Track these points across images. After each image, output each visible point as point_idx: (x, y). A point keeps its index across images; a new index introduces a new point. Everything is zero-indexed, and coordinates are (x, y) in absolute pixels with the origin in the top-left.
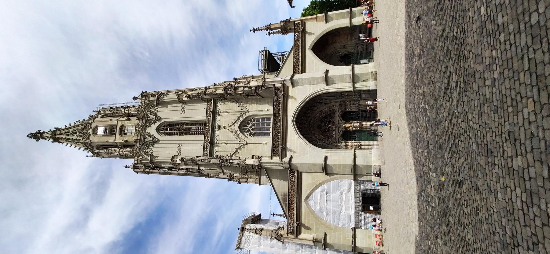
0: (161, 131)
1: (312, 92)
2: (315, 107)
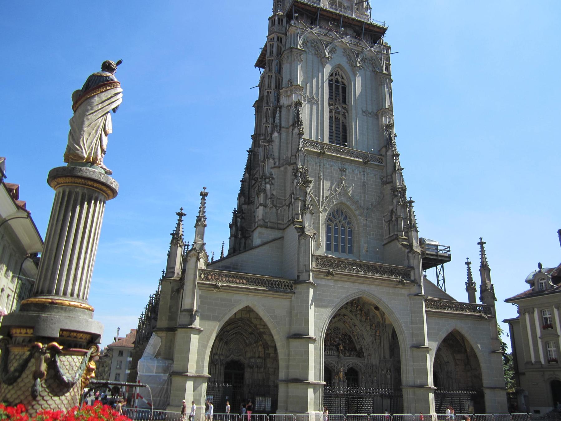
0: (336, 72)
1: (403, 325)
2: (369, 326)
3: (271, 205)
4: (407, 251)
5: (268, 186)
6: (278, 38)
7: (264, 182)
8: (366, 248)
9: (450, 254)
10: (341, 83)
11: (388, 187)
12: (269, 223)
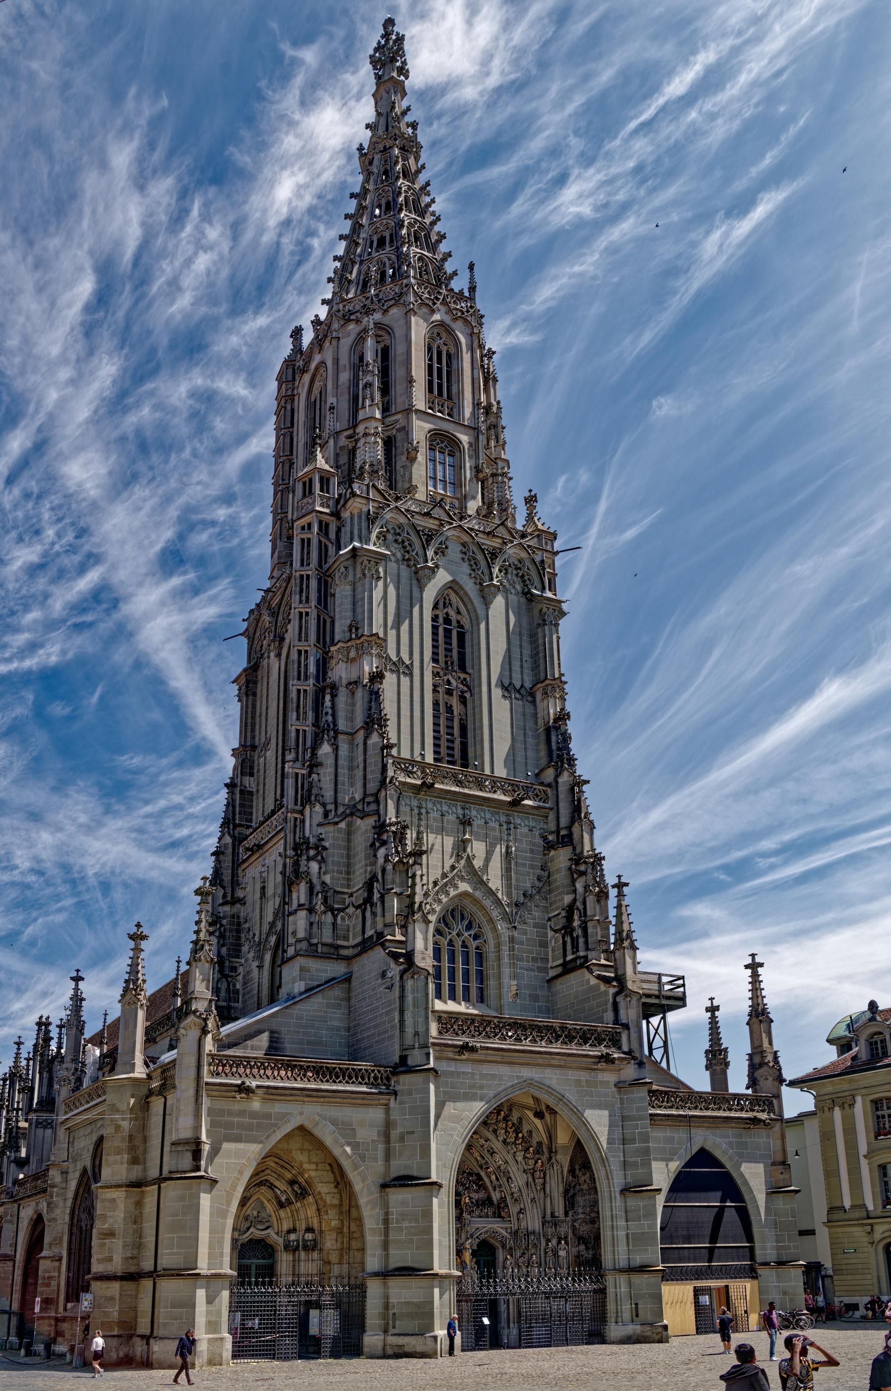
3: (323, 908)
5: (314, 866)
6: (320, 522)
7: (304, 857)
9: (684, 993)
10: (454, 623)
11: (562, 857)
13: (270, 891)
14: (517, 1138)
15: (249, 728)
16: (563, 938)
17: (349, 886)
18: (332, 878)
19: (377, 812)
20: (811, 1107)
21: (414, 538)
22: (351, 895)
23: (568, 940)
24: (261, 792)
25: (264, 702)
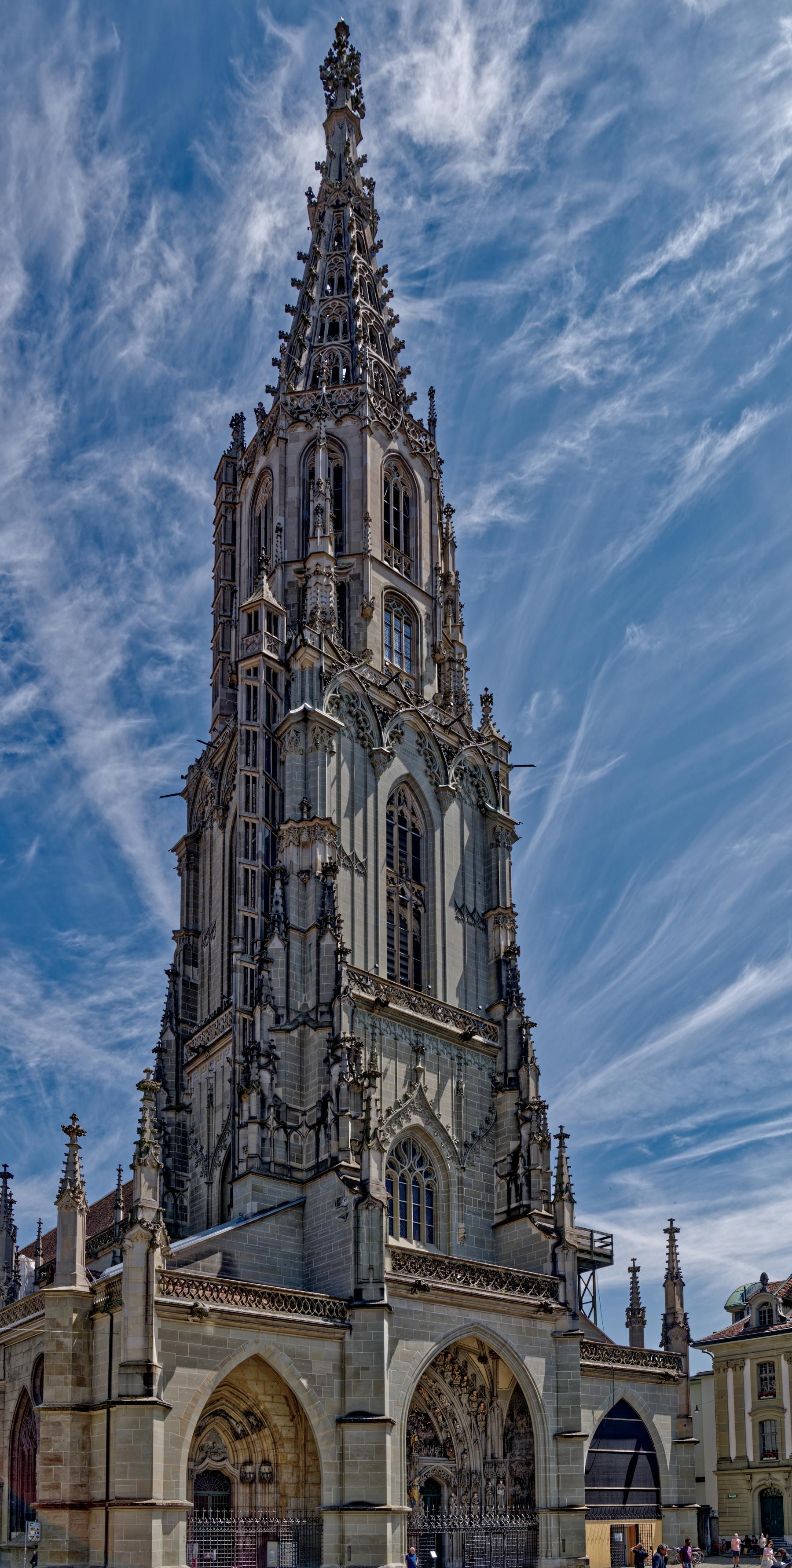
3: (275, 1124)
4: (552, 1242)
5: (266, 1076)
7: (255, 1065)
8: (462, 1231)
9: (612, 1251)
12: (272, 1165)
13: (218, 1100)
14: (462, 1380)
15: (191, 909)
16: (508, 1184)
17: (302, 1104)
18: (285, 1092)
19: (331, 1025)
20: (710, 1368)
21: (369, 713)
22: (304, 1114)
23: (513, 1187)
24: (206, 986)
25: (208, 881)
